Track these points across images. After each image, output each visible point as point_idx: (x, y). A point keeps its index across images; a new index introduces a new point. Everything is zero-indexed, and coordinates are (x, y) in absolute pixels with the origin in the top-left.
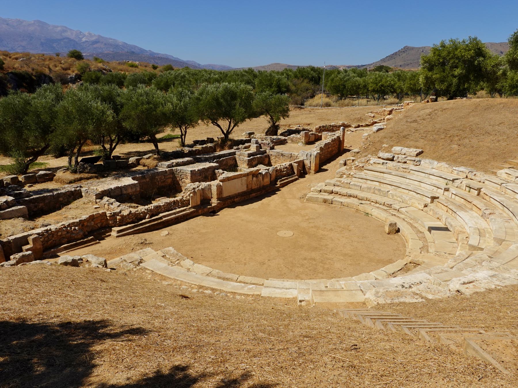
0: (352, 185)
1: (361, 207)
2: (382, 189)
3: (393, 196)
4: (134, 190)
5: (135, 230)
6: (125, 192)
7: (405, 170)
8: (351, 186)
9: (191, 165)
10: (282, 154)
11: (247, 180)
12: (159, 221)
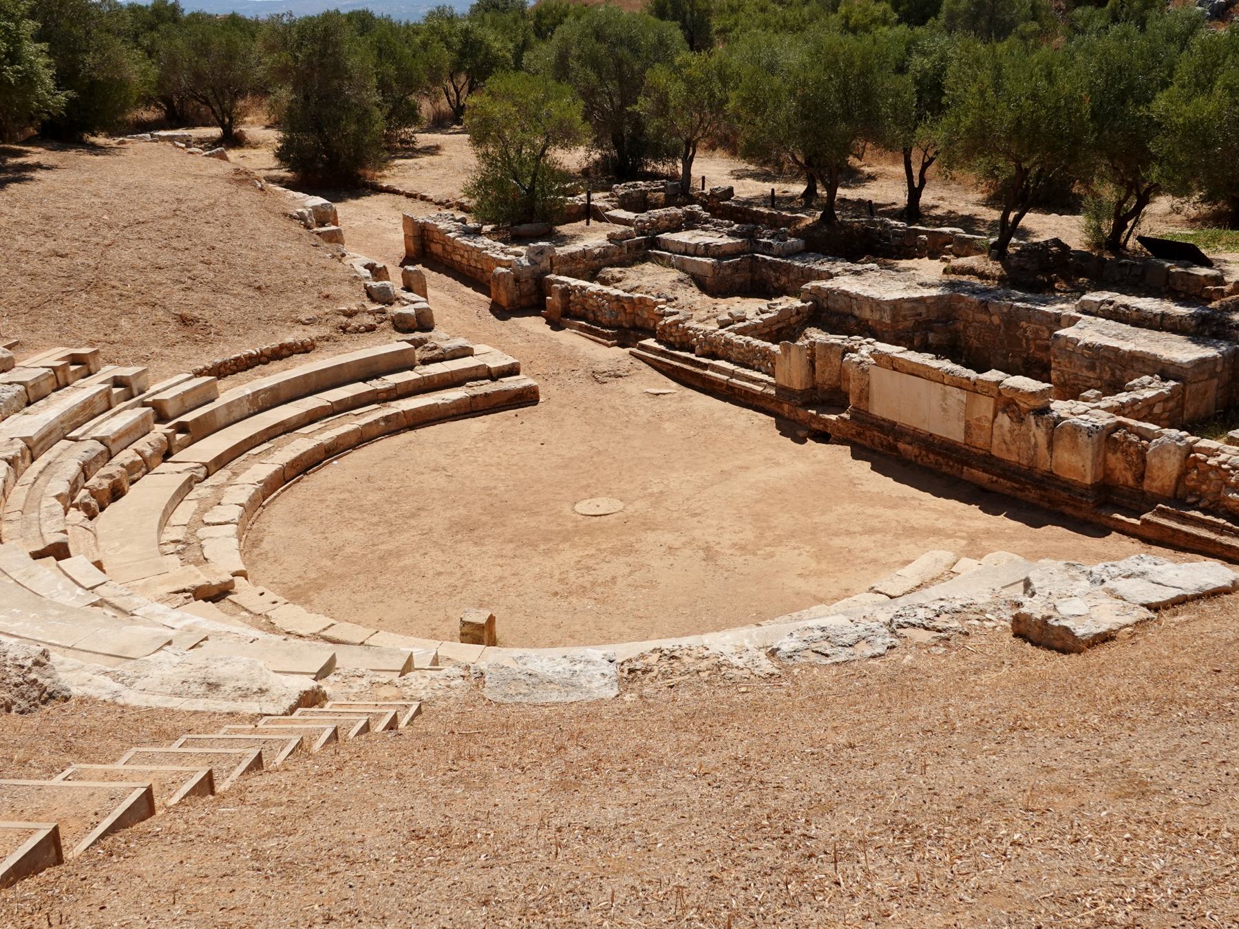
4: (877, 316)
5: (660, 362)
6: (857, 313)
9: (1144, 333)
11: (968, 407)
12: (685, 366)
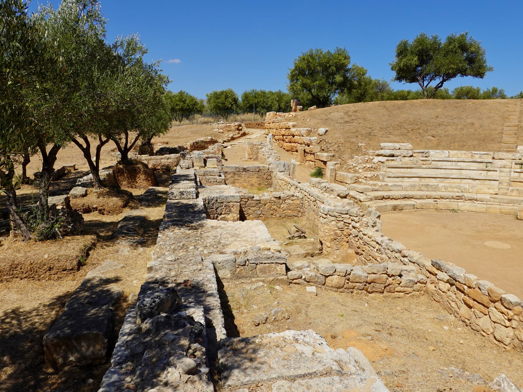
0: (391, 186)
1: (440, 206)
2: (430, 184)
3: (446, 188)
7: (424, 163)
8: (391, 188)
10: (244, 169)
